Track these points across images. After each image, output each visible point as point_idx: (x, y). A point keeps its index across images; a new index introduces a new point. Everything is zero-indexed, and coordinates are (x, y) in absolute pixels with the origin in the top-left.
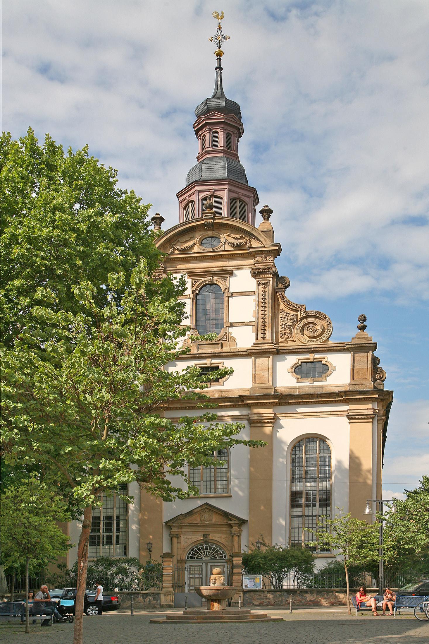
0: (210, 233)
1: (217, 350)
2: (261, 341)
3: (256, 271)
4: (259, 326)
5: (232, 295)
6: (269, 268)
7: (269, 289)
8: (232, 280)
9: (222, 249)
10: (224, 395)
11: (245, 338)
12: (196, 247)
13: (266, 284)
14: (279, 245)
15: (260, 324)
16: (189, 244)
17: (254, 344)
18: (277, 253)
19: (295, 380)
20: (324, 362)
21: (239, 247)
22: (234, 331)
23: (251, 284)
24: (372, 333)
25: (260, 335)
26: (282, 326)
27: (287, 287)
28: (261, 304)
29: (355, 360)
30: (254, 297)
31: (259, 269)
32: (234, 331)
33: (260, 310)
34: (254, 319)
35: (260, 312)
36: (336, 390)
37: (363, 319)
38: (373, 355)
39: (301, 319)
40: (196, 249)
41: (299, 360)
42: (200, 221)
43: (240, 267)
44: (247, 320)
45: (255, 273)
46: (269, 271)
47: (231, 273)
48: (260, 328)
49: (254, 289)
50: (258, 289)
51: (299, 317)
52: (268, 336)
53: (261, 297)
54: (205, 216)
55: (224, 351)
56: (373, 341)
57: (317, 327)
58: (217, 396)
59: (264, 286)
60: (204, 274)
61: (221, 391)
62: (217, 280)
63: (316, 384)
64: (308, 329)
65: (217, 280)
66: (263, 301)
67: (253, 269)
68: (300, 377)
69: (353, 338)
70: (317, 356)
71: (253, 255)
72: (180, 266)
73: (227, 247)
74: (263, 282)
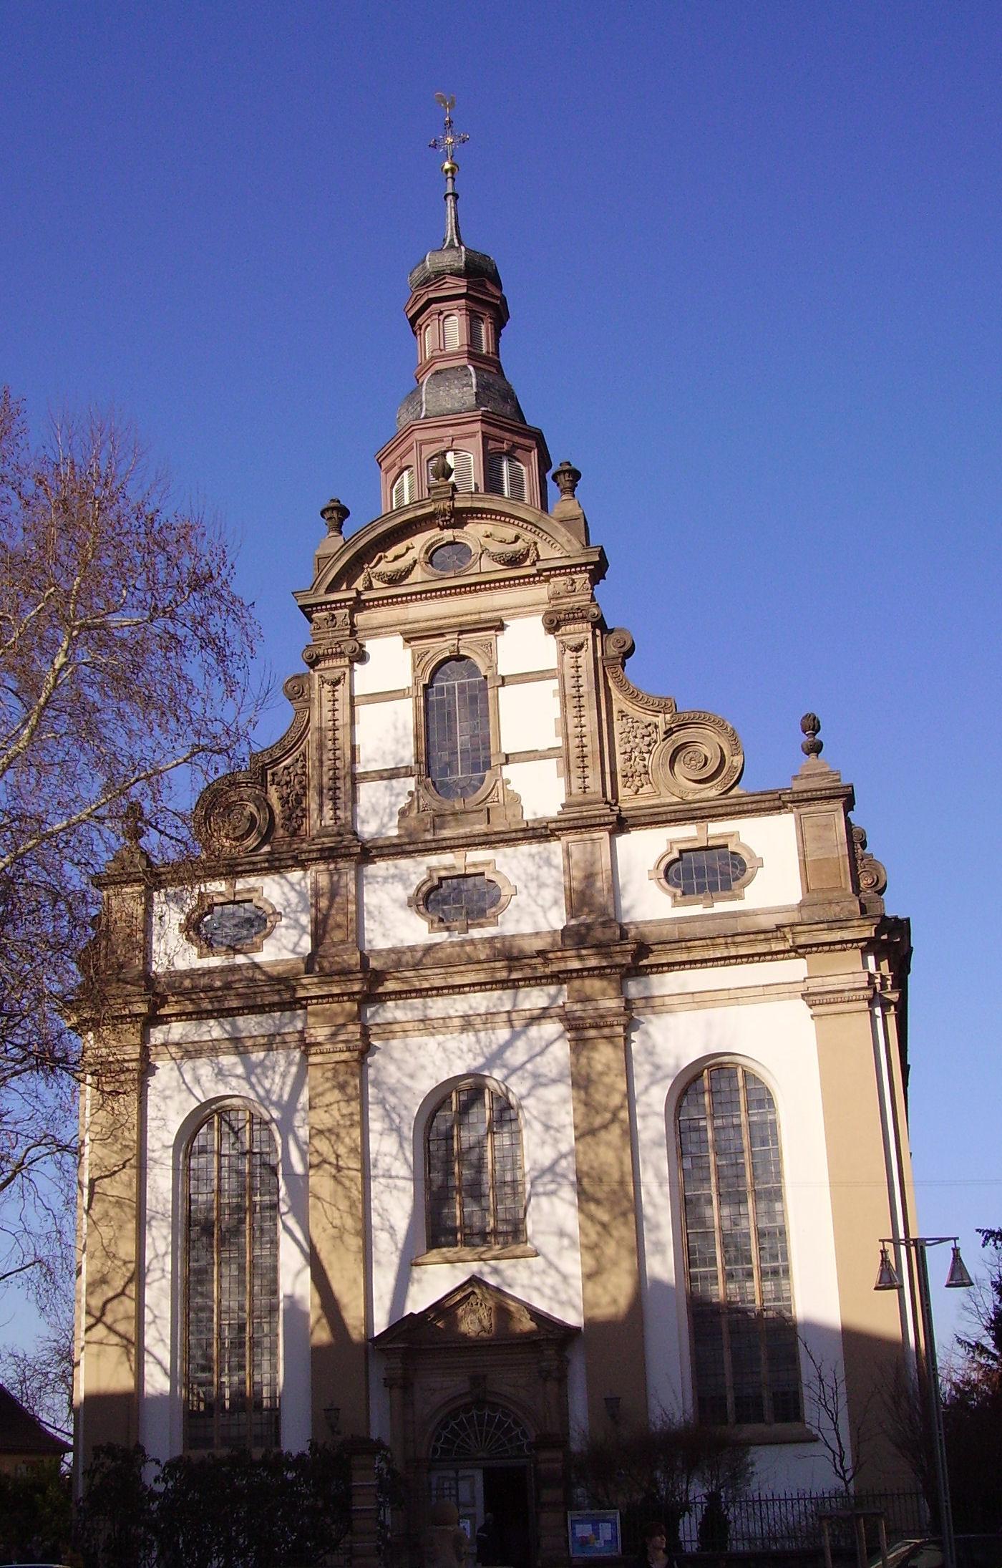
1: (481, 828)
2: (580, 799)
3: (555, 617)
5: (504, 681)
7: (586, 657)
8: (504, 642)
9: (475, 569)
11: (539, 791)
12: (418, 568)
13: (578, 649)
14: (602, 553)
15: (574, 752)
17: (563, 806)
18: (598, 571)
19: (668, 900)
20: (731, 848)
21: (514, 561)
24: (839, 761)
25: (576, 783)
26: (626, 756)
27: (629, 653)
29: (807, 836)
30: (554, 684)
31: (559, 612)
33: (569, 717)
34: (559, 742)
35: (572, 722)
36: (768, 922)
37: (812, 725)
38: (848, 822)
39: (669, 733)
40: (417, 575)
41: (671, 843)
42: (422, 507)
43: (522, 610)
44: (542, 746)
45: (552, 621)
46: (583, 617)
48: (574, 762)
50: (561, 662)
51: (662, 728)
52: (594, 783)
53: (570, 682)
54: (436, 494)
56: (845, 782)
57: (705, 750)
59: (574, 654)
62: (469, 645)
63: (721, 907)
64: (687, 758)
65: (469, 645)
66: (574, 691)
67: (547, 613)
68: (679, 892)
69: (795, 778)
70: (717, 828)
71: (543, 575)
73: (487, 564)
74: (572, 643)
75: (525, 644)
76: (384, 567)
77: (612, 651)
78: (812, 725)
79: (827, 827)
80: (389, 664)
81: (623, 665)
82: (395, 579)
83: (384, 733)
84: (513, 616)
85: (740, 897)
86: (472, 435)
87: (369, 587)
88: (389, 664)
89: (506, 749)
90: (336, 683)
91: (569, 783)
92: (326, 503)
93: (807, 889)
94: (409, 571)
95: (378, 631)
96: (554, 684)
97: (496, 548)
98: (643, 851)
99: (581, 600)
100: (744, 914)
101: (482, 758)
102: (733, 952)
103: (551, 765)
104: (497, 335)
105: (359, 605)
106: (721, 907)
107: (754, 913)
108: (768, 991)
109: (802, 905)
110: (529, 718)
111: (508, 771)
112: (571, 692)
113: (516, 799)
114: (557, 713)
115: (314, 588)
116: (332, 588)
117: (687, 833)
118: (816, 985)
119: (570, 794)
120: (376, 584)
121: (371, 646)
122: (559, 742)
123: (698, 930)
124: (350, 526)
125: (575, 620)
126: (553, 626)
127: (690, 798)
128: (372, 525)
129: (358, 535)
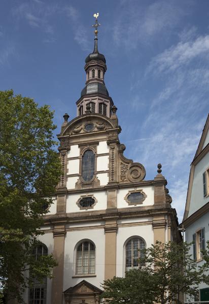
0: (89, 122)
1: (91, 188)
2: (111, 181)
4: (111, 173)
6: (115, 140)
8: (98, 147)
10: (93, 214)
14: (120, 127)
15: (111, 172)
16: (79, 129)
18: (119, 131)
19: (128, 204)
22: (99, 176)
23: (107, 150)
25: (111, 178)
27: (124, 150)
28: (112, 160)
32: (99, 176)
35: (111, 165)
36: (147, 209)
37: (160, 166)
38: (165, 187)
39: (130, 168)
40: (82, 131)
41: (130, 191)
43: (103, 140)
44: (105, 170)
47: (97, 143)
49: (108, 152)
55: (95, 188)
58: (90, 214)
60: (85, 144)
61: (92, 212)
63: (138, 206)
65: (91, 147)
70: (138, 189)
71: (107, 133)
72: (74, 141)
73: (96, 129)
75: (103, 147)
76: (76, 130)
77: (121, 149)
78: (160, 166)
79: (161, 189)
80: (75, 151)
81: (123, 152)
82: (77, 132)
83: (73, 167)
84: (100, 141)
85: (142, 203)
86: (96, 99)
87: (72, 134)
88: (75, 151)
89: (97, 170)
90: (64, 155)
91: (110, 178)
92: (64, 114)
93: (155, 202)
94: (80, 130)
95: (73, 144)
96: (108, 156)
97: (98, 126)
98: (123, 193)
99: (114, 138)
100: (142, 207)
101: (94, 173)
102: (139, 215)
103: (107, 174)
104: (104, 74)
105: (69, 138)
106: (138, 206)
107: (144, 207)
108: (145, 223)
109: (154, 206)
110: (102, 163)
111: (98, 175)
112: (111, 158)
113: (99, 181)
114: (108, 163)
115: (61, 134)
116: (64, 134)
117: (133, 189)
118: (154, 222)
119: (110, 180)
120: (73, 134)
121: (72, 147)
122: (108, 169)
123: (133, 210)
124: (69, 120)
125: (114, 142)
126: (108, 144)
127: (134, 182)
128: (73, 120)
129: (70, 122)
